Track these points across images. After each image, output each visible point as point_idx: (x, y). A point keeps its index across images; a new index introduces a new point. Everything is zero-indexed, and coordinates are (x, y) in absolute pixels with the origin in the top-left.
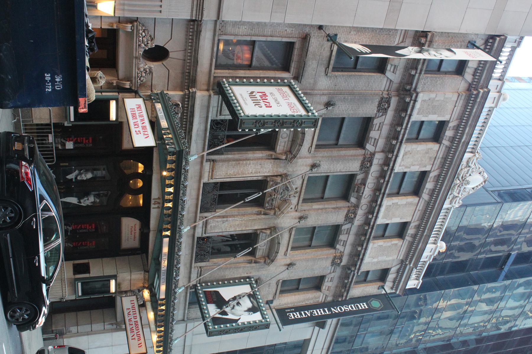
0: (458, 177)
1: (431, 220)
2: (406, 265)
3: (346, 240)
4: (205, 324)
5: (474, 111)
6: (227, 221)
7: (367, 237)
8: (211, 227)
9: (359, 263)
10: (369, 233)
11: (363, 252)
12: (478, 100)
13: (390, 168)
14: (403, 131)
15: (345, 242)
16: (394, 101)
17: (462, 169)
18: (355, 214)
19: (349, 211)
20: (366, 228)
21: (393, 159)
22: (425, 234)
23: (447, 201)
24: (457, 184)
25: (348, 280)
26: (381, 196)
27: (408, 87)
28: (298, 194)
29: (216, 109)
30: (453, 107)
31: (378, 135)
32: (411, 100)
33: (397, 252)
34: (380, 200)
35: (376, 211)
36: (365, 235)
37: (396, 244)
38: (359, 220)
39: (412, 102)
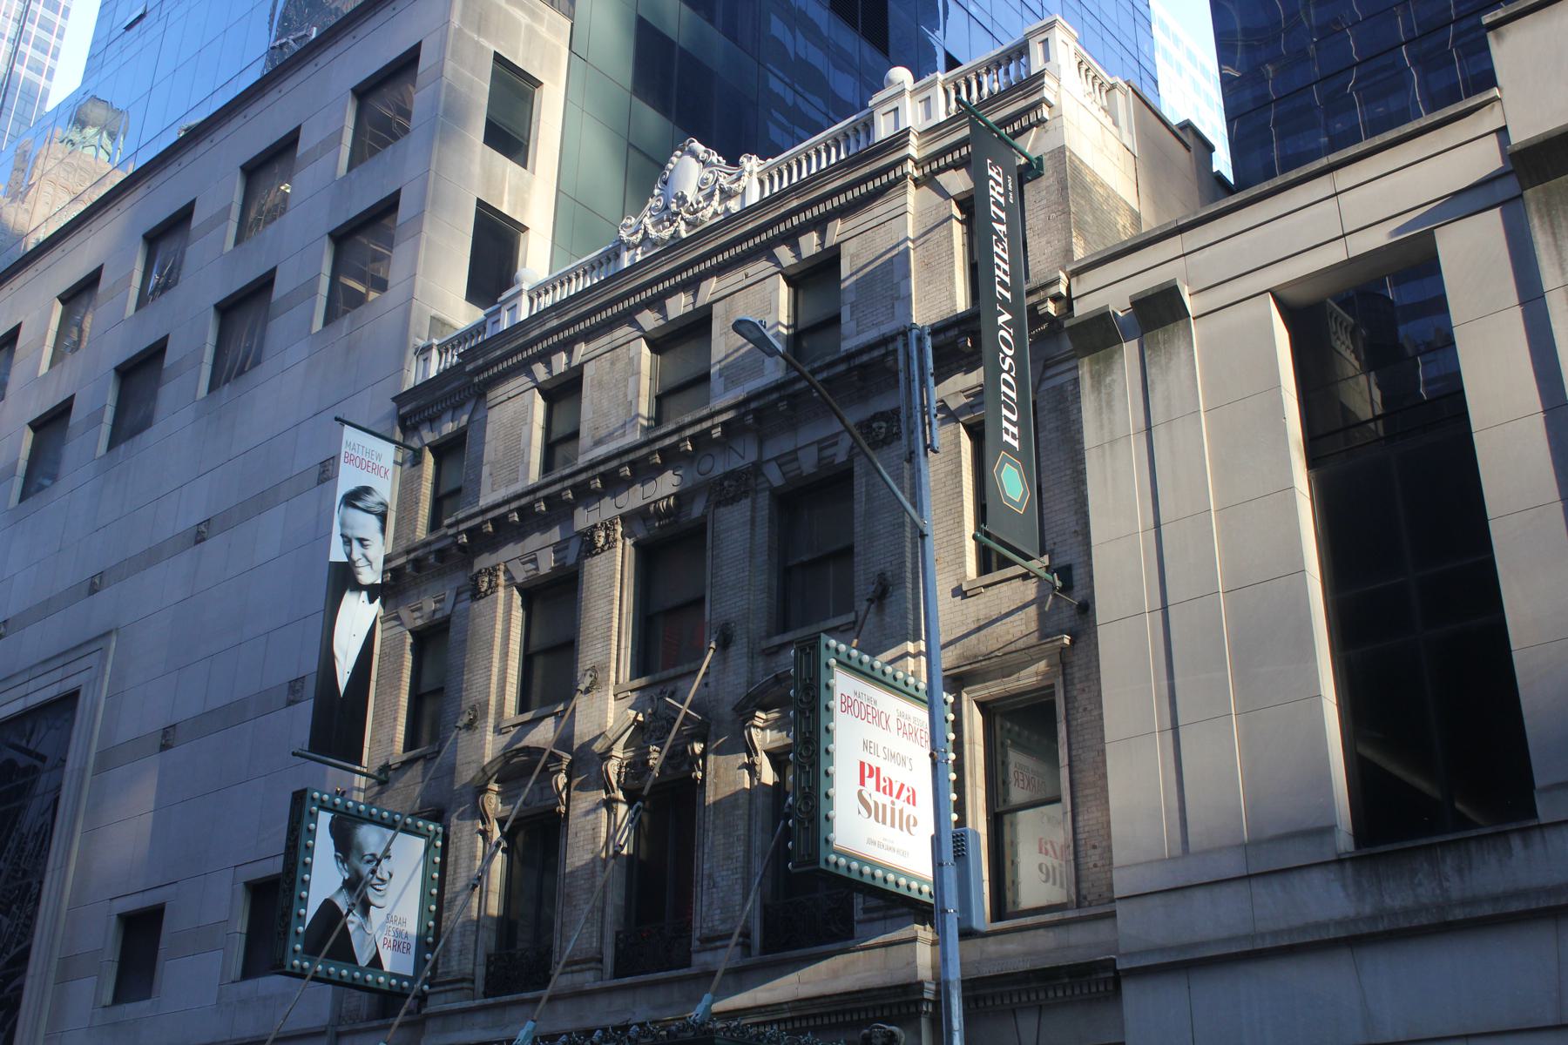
0: (672, 237)
1: (750, 226)
2: (930, 159)
3: (814, 449)
4: (315, 978)
5: (499, 353)
6: (710, 876)
7: (775, 396)
8: (723, 921)
9: (865, 358)
10: (762, 402)
11: (825, 375)
12: (480, 362)
13: (590, 474)
14: (514, 505)
15: (822, 445)
16: (484, 561)
17: (655, 245)
18: (727, 476)
19: (718, 504)
20: (750, 419)
21: (569, 482)
22: (795, 203)
23: (734, 206)
24: (688, 223)
25: (958, 337)
26: (658, 445)
27: (454, 550)
28: (670, 688)
29: (450, 995)
30: (510, 404)
31: (540, 552)
32: (460, 533)
33: (882, 229)
34: (667, 442)
35: (698, 428)
36: (775, 403)
37: (852, 256)
38: (743, 455)
39: (463, 527)
